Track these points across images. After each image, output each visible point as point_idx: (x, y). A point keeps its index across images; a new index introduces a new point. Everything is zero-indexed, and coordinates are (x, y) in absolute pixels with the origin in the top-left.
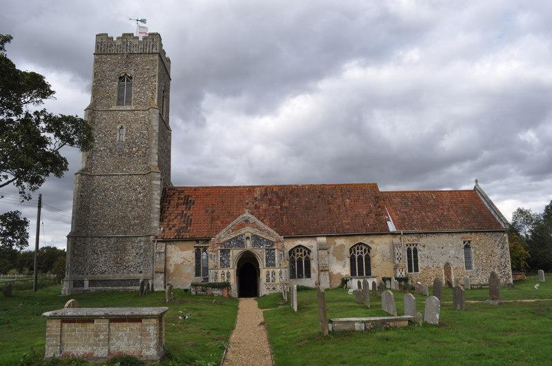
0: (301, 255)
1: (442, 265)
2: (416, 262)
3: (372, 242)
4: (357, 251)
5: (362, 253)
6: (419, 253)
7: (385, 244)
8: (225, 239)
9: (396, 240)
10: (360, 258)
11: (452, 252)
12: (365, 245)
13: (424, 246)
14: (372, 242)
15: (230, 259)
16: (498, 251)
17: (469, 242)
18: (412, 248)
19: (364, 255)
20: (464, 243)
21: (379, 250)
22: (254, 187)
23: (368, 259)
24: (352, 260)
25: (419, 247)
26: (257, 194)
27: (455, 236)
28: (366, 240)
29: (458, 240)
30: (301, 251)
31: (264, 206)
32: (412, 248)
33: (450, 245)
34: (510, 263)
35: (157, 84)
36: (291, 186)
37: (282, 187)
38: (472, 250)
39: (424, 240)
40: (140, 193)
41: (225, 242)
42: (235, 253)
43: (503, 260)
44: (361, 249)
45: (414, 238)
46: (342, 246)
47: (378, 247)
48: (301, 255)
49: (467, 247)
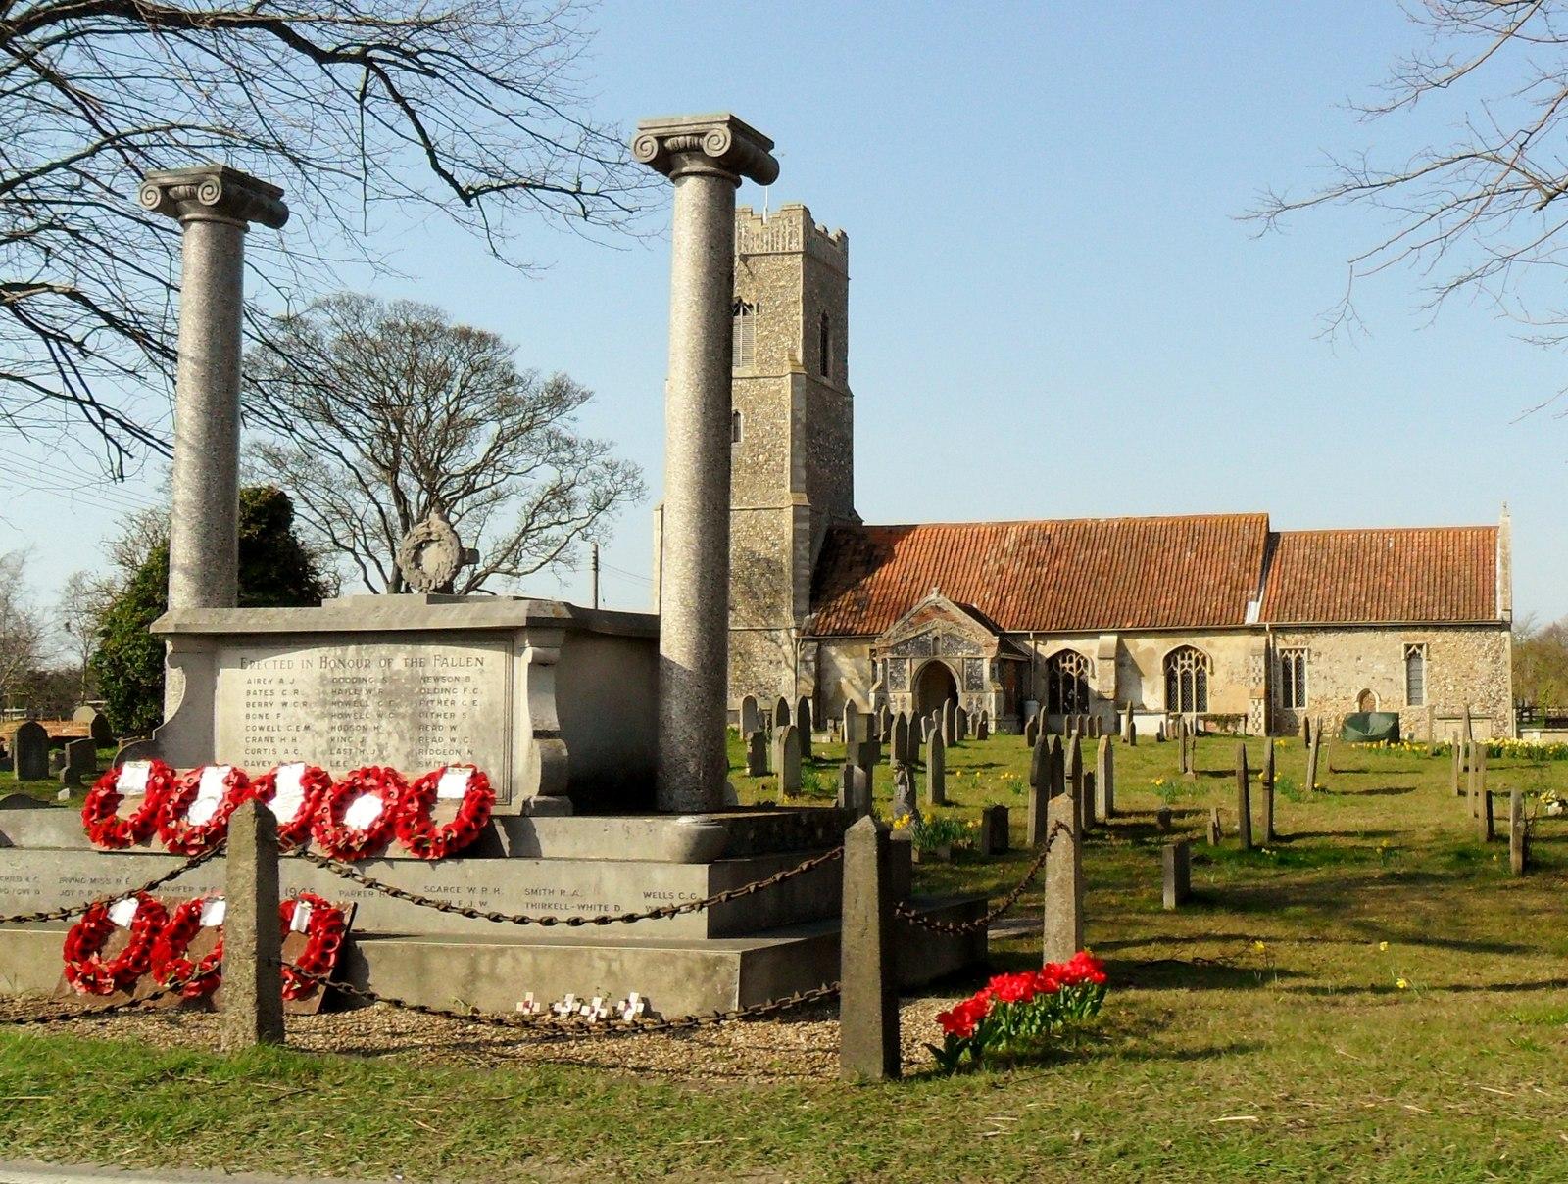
0: (1071, 669)
1: (1355, 695)
2: (1300, 686)
3: (1210, 645)
4: (1180, 662)
5: (1190, 666)
6: (1307, 668)
7: (1237, 647)
8: (897, 640)
9: (1259, 641)
10: (1186, 677)
11: (1381, 667)
12: (1196, 651)
13: (1319, 655)
14: (1210, 645)
15: (907, 674)
16: (1484, 667)
17: (1420, 647)
18: (1293, 658)
19: (1193, 672)
20: (1409, 647)
21: (1223, 661)
22: (1008, 525)
23: (1201, 678)
24: (1170, 677)
25: (1305, 656)
26: (1009, 543)
27: (1388, 635)
28: (1198, 642)
29: (1395, 643)
30: (1071, 661)
31: (1018, 567)
32: (1293, 658)
33: (1377, 653)
34: (1510, 694)
35: (800, 319)
36: (1082, 523)
37: (1063, 526)
38: (1425, 664)
39: (1320, 641)
40: (774, 545)
41: (897, 645)
42: (911, 667)
43: (1494, 687)
44: (1190, 658)
45: (1298, 636)
46: (1151, 652)
47: (1222, 656)
48: (1071, 669)
49: (1412, 657)
